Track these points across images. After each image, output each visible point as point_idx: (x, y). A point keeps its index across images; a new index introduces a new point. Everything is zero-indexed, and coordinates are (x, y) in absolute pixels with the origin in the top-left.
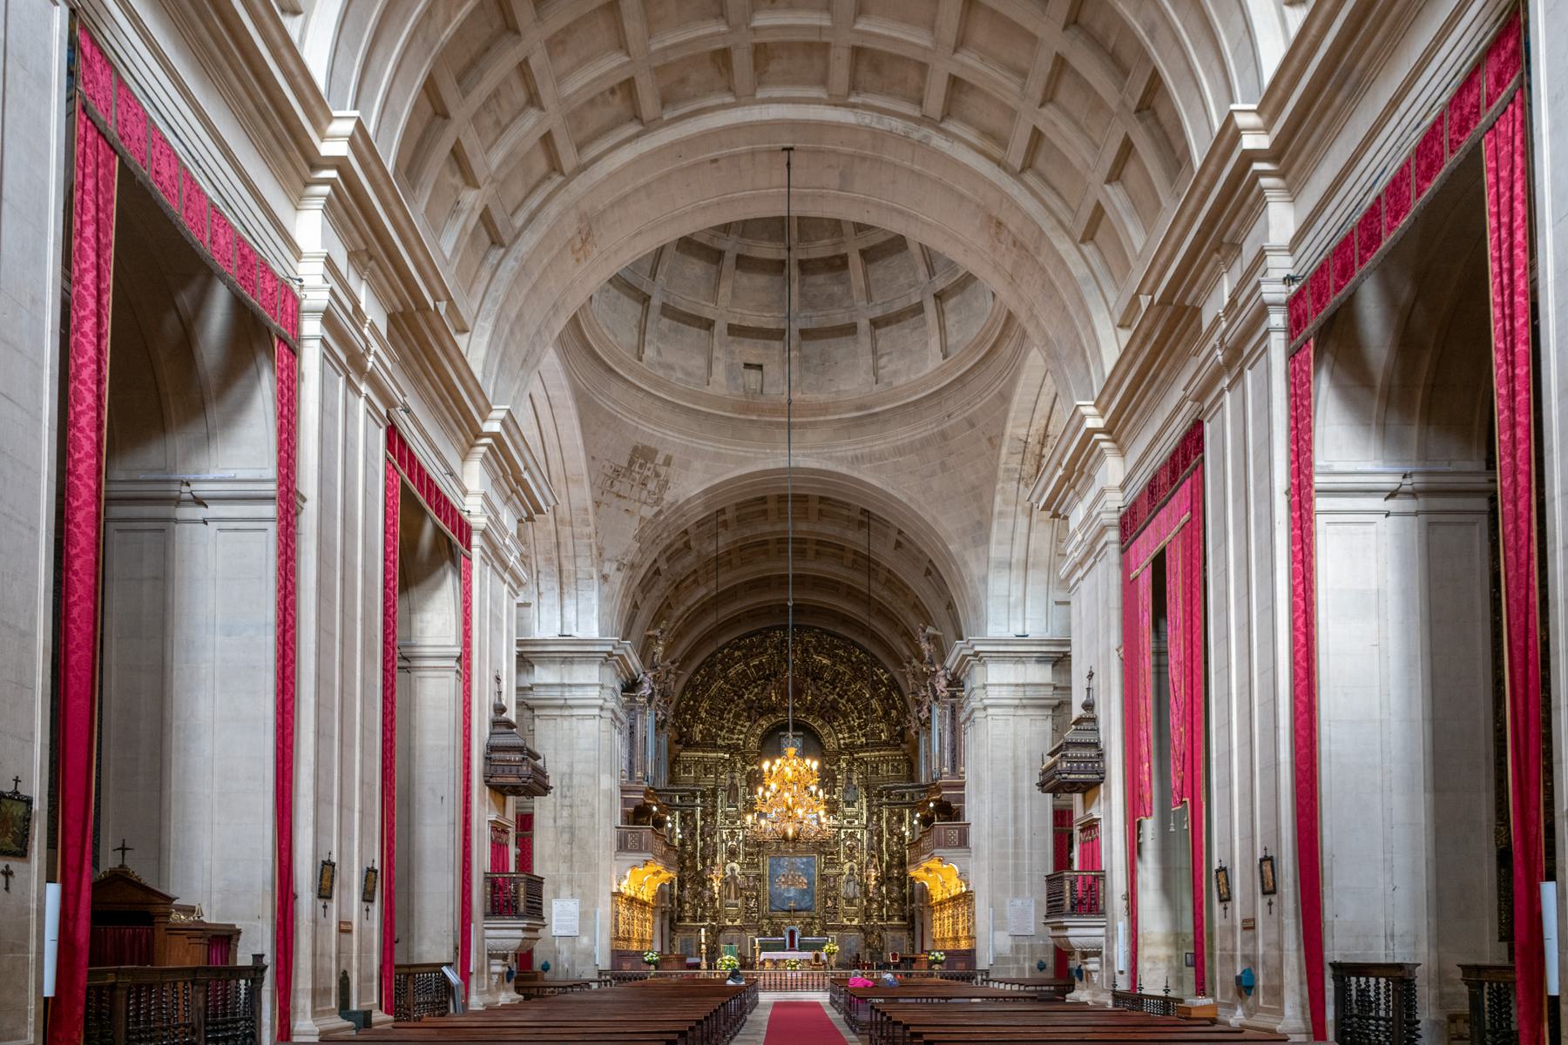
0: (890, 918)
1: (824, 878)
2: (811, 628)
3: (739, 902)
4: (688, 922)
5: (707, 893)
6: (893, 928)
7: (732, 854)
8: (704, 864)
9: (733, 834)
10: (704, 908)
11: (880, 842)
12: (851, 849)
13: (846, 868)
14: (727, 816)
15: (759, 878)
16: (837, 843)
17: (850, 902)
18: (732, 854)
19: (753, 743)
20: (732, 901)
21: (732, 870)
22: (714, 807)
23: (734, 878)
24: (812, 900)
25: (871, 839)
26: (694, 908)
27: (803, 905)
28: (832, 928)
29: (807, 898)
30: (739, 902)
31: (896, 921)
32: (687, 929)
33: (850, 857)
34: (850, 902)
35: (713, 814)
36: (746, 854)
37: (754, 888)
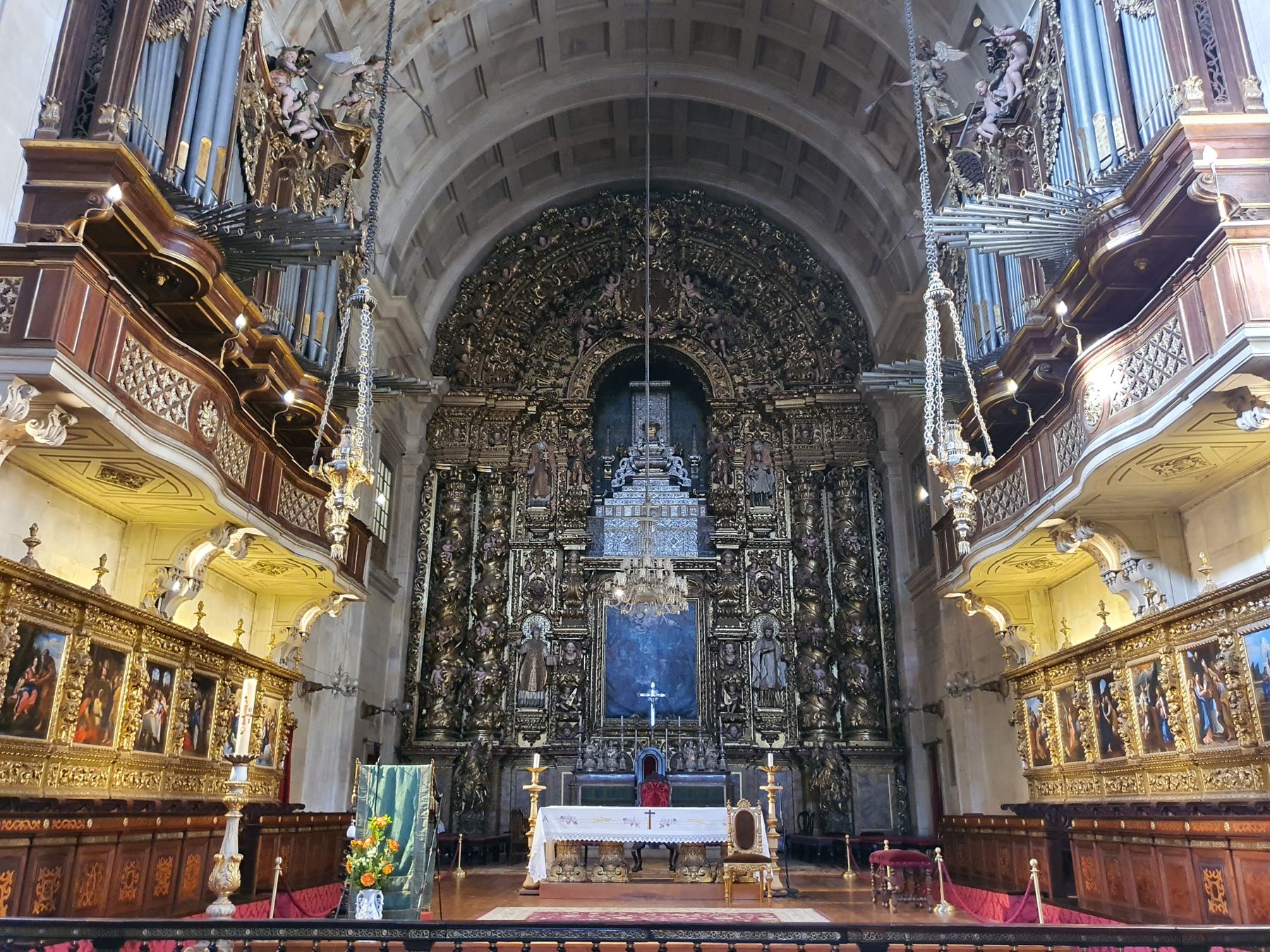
0: (850, 732)
1: (714, 646)
2: (684, 188)
3: (545, 696)
5: (481, 677)
7: (537, 595)
9: (538, 552)
11: (821, 569)
12: (766, 586)
13: (757, 627)
16: (737, 573)
19: (582, 384)
20: (530, 694)
21: (535, 628)
23: (537, 644)
25: (801, 566)
26: (454, 707)
28: (733, 755)
34: (768, 696)
36: (562, 596)
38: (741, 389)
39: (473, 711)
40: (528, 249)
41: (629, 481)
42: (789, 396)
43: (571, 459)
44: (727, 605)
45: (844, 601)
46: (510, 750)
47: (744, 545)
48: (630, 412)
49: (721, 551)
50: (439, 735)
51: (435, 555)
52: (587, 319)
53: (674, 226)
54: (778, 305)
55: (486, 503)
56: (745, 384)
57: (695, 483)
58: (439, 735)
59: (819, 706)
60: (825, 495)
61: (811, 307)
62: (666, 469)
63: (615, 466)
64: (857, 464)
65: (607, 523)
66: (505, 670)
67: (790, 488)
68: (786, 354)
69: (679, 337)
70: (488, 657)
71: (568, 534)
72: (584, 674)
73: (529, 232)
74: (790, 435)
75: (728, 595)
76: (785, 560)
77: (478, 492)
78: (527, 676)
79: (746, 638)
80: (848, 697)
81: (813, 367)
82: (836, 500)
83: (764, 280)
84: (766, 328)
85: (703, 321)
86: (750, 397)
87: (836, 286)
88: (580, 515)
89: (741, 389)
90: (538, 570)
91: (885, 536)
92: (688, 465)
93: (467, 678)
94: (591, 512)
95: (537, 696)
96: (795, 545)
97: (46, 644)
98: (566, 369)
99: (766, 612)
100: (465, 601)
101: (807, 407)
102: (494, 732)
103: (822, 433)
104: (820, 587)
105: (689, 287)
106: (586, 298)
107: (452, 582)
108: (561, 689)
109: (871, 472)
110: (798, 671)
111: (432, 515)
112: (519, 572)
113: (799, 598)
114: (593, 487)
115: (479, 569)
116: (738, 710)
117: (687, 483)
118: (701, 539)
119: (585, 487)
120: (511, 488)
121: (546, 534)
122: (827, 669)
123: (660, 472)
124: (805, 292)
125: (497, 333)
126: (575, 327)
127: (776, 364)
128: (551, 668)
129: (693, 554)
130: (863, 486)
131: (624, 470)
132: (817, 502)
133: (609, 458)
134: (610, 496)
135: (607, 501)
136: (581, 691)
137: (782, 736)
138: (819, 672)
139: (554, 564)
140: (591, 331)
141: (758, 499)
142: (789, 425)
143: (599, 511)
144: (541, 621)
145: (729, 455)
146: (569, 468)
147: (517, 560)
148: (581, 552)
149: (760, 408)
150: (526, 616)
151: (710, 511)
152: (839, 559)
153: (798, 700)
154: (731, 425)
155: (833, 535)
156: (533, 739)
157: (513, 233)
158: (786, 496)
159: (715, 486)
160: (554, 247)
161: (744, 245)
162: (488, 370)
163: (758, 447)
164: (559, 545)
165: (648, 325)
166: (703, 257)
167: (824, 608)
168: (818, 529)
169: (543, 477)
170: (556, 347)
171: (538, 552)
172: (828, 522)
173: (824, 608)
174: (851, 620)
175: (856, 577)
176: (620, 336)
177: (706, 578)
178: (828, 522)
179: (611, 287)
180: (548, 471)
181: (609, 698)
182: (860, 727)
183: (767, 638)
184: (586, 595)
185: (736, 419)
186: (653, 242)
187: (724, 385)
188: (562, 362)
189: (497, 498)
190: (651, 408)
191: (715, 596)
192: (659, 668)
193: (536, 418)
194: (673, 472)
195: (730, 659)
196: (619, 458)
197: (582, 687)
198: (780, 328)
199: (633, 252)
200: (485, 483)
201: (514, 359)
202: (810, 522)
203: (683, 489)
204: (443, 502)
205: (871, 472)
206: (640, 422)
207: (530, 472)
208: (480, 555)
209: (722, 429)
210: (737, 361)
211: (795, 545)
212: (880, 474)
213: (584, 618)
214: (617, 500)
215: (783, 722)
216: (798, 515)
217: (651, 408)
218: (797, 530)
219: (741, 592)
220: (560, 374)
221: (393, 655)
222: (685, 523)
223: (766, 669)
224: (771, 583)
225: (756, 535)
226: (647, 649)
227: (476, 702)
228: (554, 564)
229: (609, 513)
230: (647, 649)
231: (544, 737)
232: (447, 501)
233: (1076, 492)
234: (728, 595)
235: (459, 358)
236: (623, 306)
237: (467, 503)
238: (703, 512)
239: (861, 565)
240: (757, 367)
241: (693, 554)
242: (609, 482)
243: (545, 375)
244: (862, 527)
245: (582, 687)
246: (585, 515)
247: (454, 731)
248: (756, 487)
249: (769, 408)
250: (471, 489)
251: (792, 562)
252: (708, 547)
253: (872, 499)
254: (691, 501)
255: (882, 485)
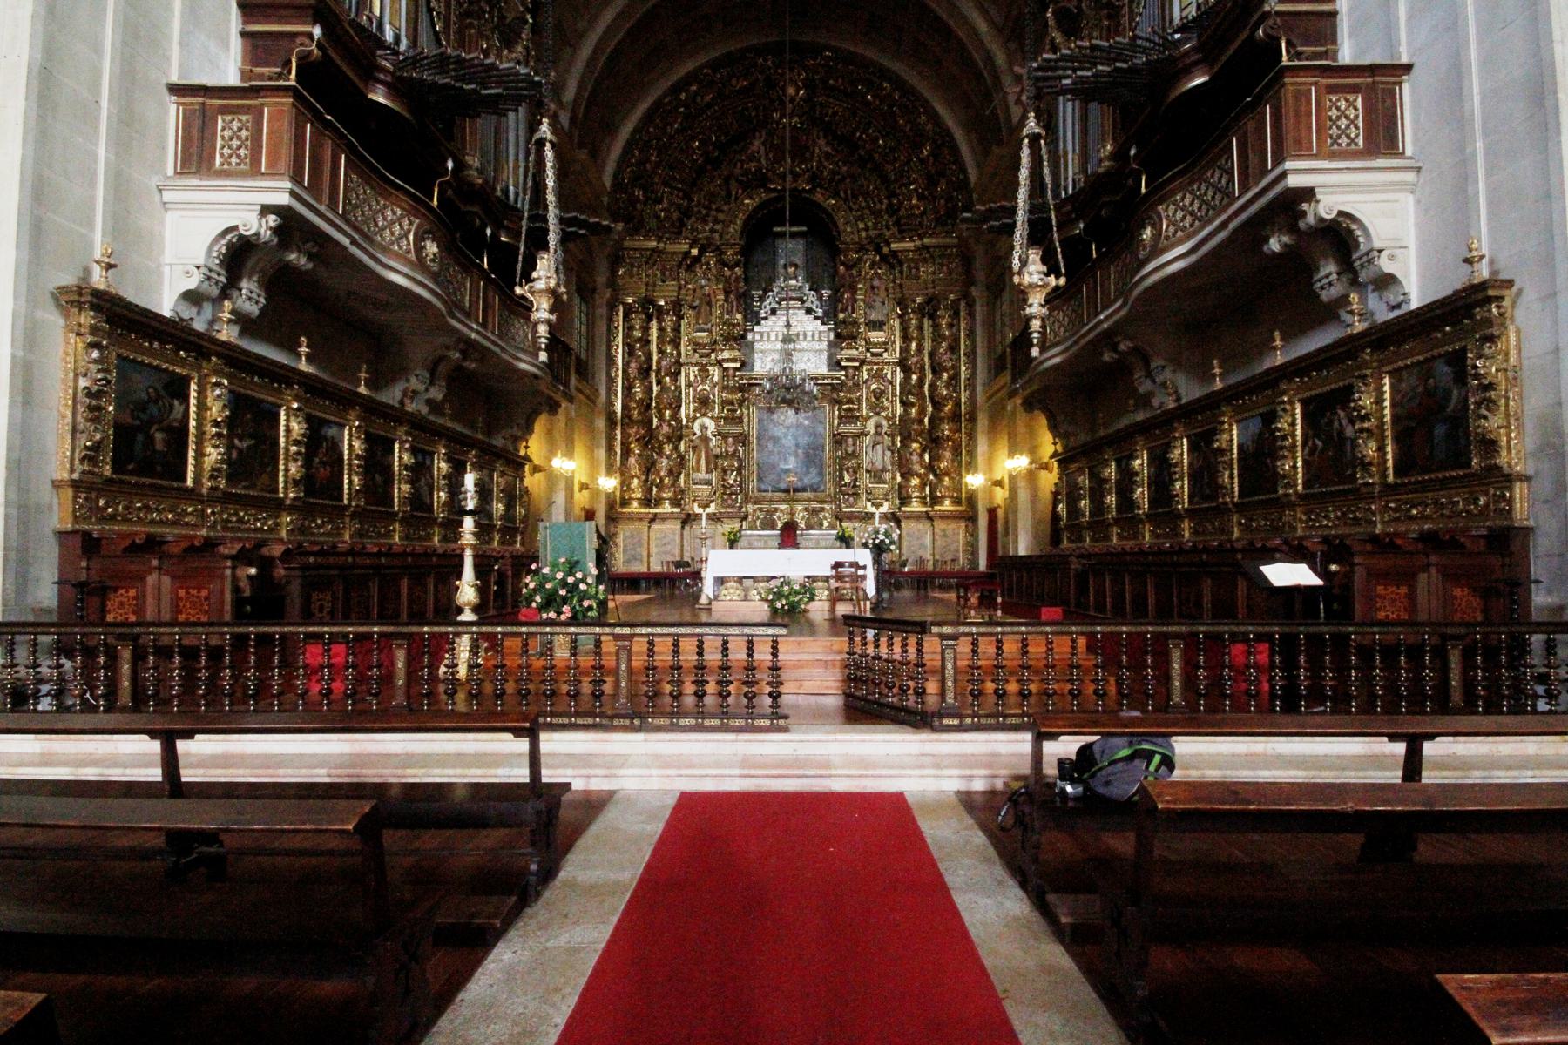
0: (935, 500)
1: (838, 440)
3: (714, 477)
4: (635, 507)
6: (946, 517)
7: (704, 403)
8: (661, 419)
9: (703, 369)
10: (661, 486)
11: (921, 381)
12: (879, 394)
13: (871, 427)
14: (696, 344)
15: (742, 439)
16: (856, 385)
17: (877, 476)
18: (704, 403)
20: (702, 475)
21: (704, 428)
22: (677, 329)
23: (705, 439)
24: (821, 474)
25: (907, 379)
27: (806, 481)
28: (851, 517)
29: (814, 471)
30: (714, 477)
31: (947, 506)
32: (632, 518)
33: (876, 409)
34: (877, 476)
35: (677, 345)
36: (724, 403)
37: (735, 454)
38: (863, 234)
39: (661, 486)
40: (687, 107)
41: (773, 312)
42: (902, 240)
43: (727, 293)
44: (850, 410)
45: (937, 406)
46: (689, 515)
47: (863, 362)
48: (775, 253)
49: (845, 368)
50: (635, 504)
51: (624, 371)
52: (737, 171)
53: (809, 85)
54: (896, 160)
55: (661, 329)
56: (867, 229)
57: (826, 313)
58: (635, 504)
59: (915, 481)
60: (927, 323)
61: (922, 161)
62: (803, 302)
63: (762, 299)
64: (952, 297)
65: (757, 346)
66: (682, 457)
67: (900, 316)
68: (900, 204)
69: (814, 188)
70: (668, 449)
71: (726, 355)
72: (740, 460)
73: (687, 91)
74: (901, 272)
75: (850, 401)
76: (894, 373)
77: (654, 324)
78: (698, 462)
79: (864, 434)
80: (936, 475)
81: (924, 213)
82: (936, 326)
83: (883, 137)
84: (885, 180)
85: (833, 173)
86: (871, 240)
87: (945, 141)
88: (735, 339)
89: (863, 234)
90: (703, 382)
91: (972, 355)
92: (820, 298)
93: (654, 463)
94: (744, 337)
95: (707, 477)
96: (903, 363)
97: (332, 432)
98: (721, 216)
99: (878, 414)
100: (649, 406)
101: (917, 249)
102: (676, 502)
103: (926, 272)
104: (920, 396)
105: (822, 142)
106: (736, 152)
107: (638, 391)
108: (724, 471)
109: (963, 304)
110: (900, 457)
111: (620, 339)
112: (689, 385)
113: (903, 403)
114: (745, 317)
115: (659, 383)
116: (855, 486)
117: (820, 312)
118: (830, 357)
119: (739, 316)
120: (680, 317)
121: (708, 356)
122: (921, 456)
123: (798, 304)
124: (918, 147)
125: (665, 184)
126: (727, 180)
127: (892, 210)
128: (717, 456)
129: (823, 370)
130: (956, 315)
131: (769, 303)
132: (920, 328)
133: (756, 293)
134: (758, 323)
135: (757, 328)
136: (739, 473)
137: (886, 505)
138: (915, 458)
139: (716, 379)
140: (740, 182)
141: (877, 325)
142: (901, 263)
143: (750, 336)
144: (708, 422)
145: (854, 290)
146: (726, 301)
147: (687, 375)
148: (736, 369)
149: (878, 250)
150: (695, 418)
151: (838, 336)
152: (934, 372)
153: (899, 479)
154: (854, 265)
155: (931, 355)
156: (705, 506)
157: (675, 89)
158: (897, 323)
159: (841, 316)
160: (709, 106)
161: (868, 103)
162: (658, 217)
163: (876, 283)
164: (719, 363)
165: (789, 178)
166: (835, 114)
167: (922, 411)
168: (920, 349)
169: (704, 308)
170: (712, 196)
171: (703, 369)
172: (928, 345)
173: (922, 411)
174: (942, 420)
175: (947, 388)
176: (764, 186)
177: (834, 388)
178: (928, 345)
179: (757, 143)
180: (709, 304)
181: (760, 479)
182: (943, 497)
183: (877, 433)
184: (741, 402)
185: (860, 259)
186: (792, 100)
187: (852, 229)
188: (719, 210)
189: (669, 323)
190: (791, 250)
191: (839, 402)
192: (797, 456)
193: (697, 259)
194: (808, 304)
195: (850, 450)
196: (766, 291)
197: (740, 470)
198: (896, 181)
199: (776, 110)
200: (660, 312)
201: (679, 207)
202: (914, 345)
203: (816, 318)
204: (629, 329)
205: (963, 304)
206: (782, 262)
207: (697, 303)
208: (658, 371)
209: (849, 268)
210: (861, 209)
211: (903, 363)
212: (971, 306)
213: (741, 418)
214: (765, 327)
215: (887, 494)
216: (906, 338)
217: (791, 250)
218: (905, 350)
219: (859, 400)
220: (716, 221)
221: (598, 447)
222: (817, 346)
223: (876, 456)
224: (882, 393)
225: (873, 355)
226: (789, 442)
227: (662, 481)
228: (716, 379)
229: (758, 337)
230: (789, 442)
231: (713, 506)
232: (631, 328)
233: (1123, 312)
234: (850, 401)
235: (634, 208)
236: (767, 159)
237: (646, 329)
238: (832, 336)
239: (950, 378)
240: (876, 214)
241: (823, 370)
242: (757, 313)
243: (706, 222)
244: (954, 348)
245: (740, 470)
246: (738, 339)
247: (647, 501)
248: (873, 316)
249: (886, 250)
250: (650, 318)
251: (900, 375)
252: (835, 364)
253: (963, 325)
254: (824, 328)
255: (971, 315)
